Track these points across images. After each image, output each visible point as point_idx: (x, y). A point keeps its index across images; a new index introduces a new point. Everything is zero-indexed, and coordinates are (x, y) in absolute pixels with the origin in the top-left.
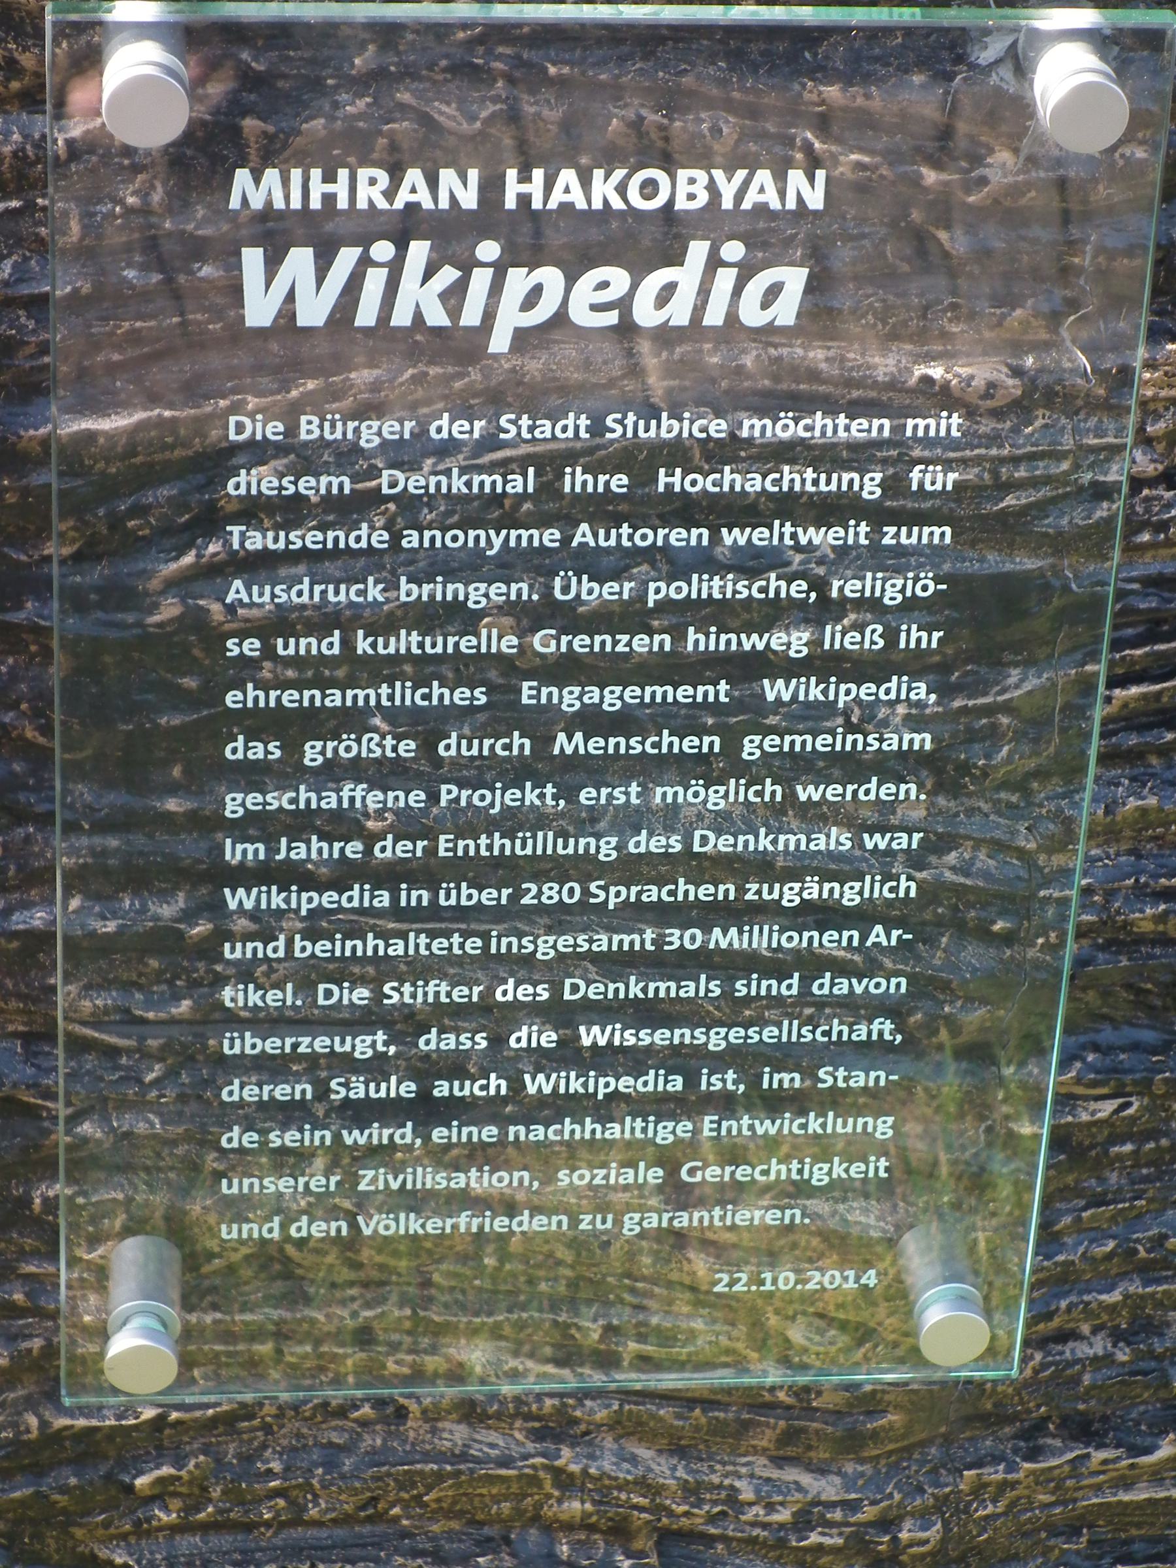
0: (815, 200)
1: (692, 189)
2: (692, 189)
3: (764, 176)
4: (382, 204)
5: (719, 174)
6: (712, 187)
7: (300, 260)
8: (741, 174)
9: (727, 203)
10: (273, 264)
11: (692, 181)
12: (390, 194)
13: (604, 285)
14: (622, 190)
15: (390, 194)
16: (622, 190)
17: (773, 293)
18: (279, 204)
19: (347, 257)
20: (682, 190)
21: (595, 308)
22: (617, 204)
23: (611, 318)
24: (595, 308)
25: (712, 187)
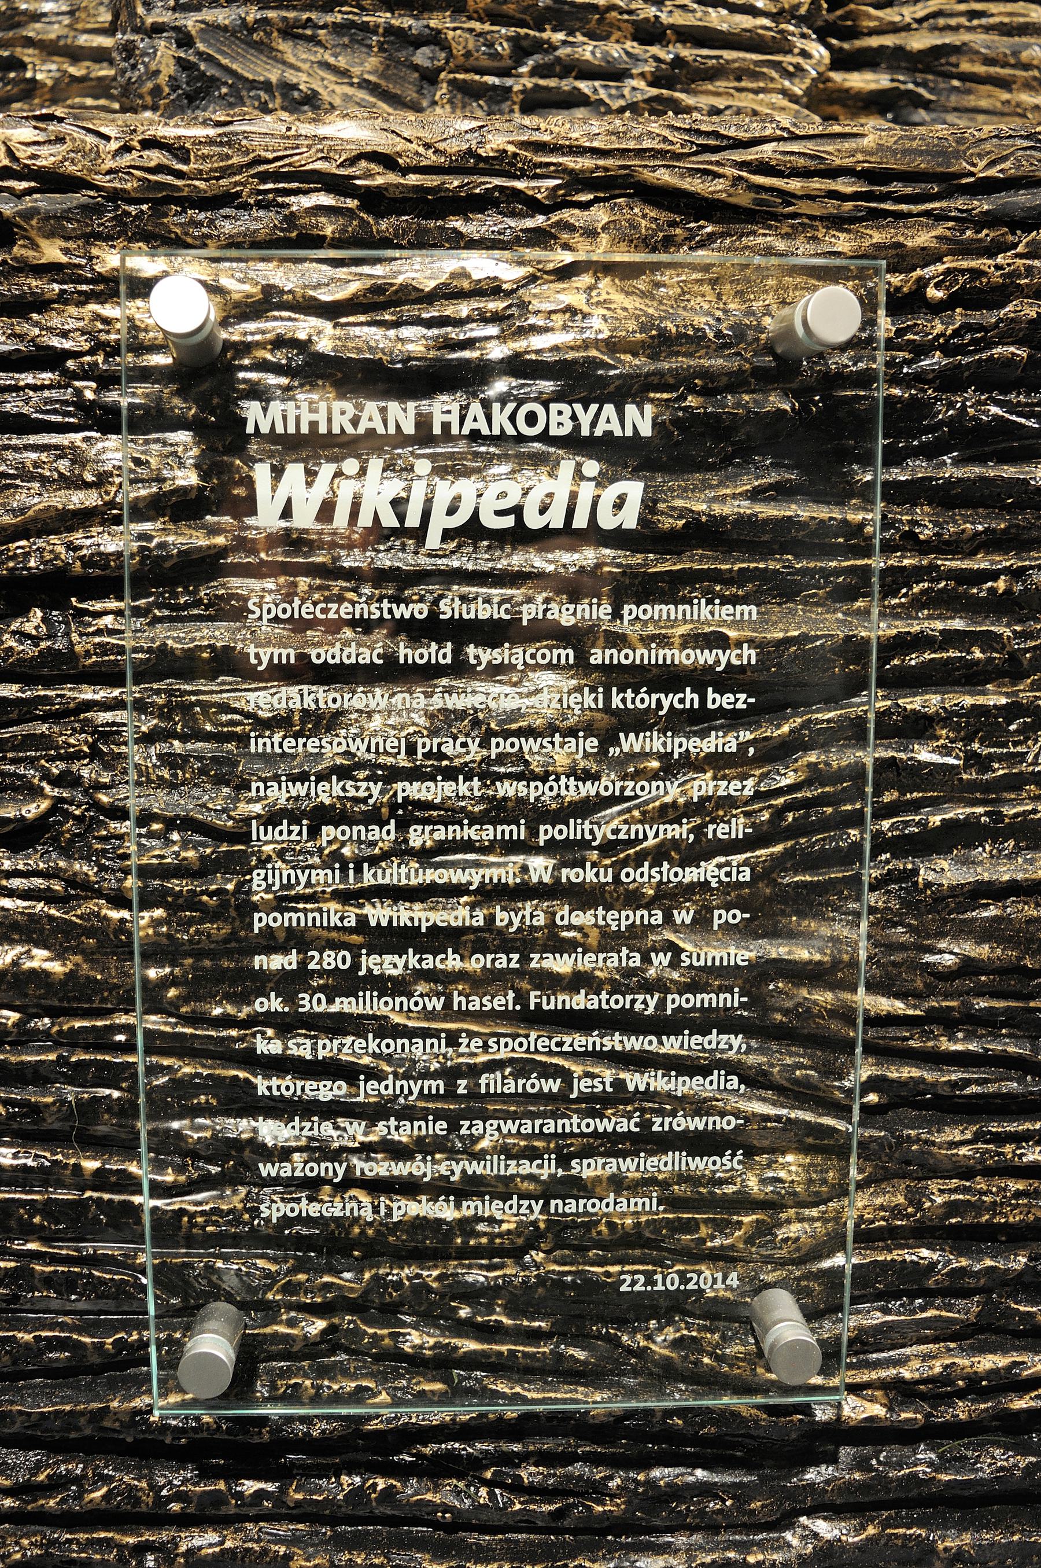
0: (646, 430)
1: (560, 419)
2: (560, 419)
3: (609, 409)
4: (350, 430)
5: (578, 407)
6: (574, 417)
7: (295, 471)
8: (594, 407)
9: (585, 432)
10: (277, 472)
11: (560, 413)
12: (355, 422)
13: (503, 495)
14: (512, 418)
15: (355, 422)
16: (512, 418)
17: (619, 504)
18: (280, 430)
19: (327, 470)
20: (554, 418)
21: (499, 513)
22: (510, 431)
23: (509, 522)
24: (499, 513)
25: (574, 417)
